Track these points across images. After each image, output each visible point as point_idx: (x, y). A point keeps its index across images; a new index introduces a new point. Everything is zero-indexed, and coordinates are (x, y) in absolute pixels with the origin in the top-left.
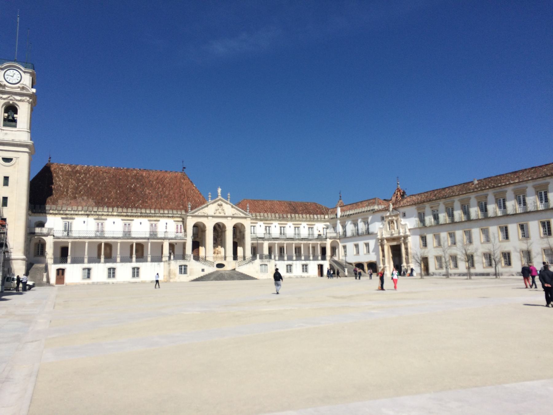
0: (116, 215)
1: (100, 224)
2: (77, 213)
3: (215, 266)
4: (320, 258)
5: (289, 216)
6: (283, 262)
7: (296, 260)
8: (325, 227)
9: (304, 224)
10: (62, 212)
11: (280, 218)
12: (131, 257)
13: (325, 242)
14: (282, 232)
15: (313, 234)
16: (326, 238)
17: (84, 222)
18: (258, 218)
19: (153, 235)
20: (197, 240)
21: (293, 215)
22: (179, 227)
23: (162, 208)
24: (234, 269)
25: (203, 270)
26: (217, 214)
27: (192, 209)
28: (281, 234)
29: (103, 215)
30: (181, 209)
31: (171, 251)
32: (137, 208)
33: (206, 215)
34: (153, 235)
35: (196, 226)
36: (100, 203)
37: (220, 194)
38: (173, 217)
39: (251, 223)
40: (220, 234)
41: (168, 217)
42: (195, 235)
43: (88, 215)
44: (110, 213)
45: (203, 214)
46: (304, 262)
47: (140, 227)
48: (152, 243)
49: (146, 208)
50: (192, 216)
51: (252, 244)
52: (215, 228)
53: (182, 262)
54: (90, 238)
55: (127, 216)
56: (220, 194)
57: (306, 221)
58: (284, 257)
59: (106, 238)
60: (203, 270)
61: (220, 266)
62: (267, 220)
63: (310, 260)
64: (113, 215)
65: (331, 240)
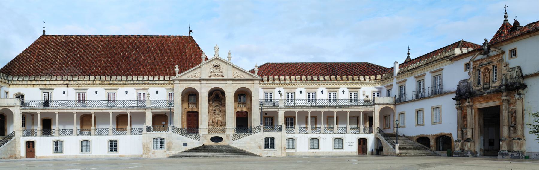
0: (97, 84)
1: (81, 94)
2: (56, 83)
8: (376, 90)
9: (343, 87)
10: (40, 82)
13: (370, 109)
15: (356, 100)
16: (374, 105)
17: (64, 92)
21: (327, 77)
29: (83, 84)
38: (164, 84)
41: (158, 84)
43: (67, 85)
44: (91, 82)
55: (112, 84)
64: (94, 84)
65: (382, 107)
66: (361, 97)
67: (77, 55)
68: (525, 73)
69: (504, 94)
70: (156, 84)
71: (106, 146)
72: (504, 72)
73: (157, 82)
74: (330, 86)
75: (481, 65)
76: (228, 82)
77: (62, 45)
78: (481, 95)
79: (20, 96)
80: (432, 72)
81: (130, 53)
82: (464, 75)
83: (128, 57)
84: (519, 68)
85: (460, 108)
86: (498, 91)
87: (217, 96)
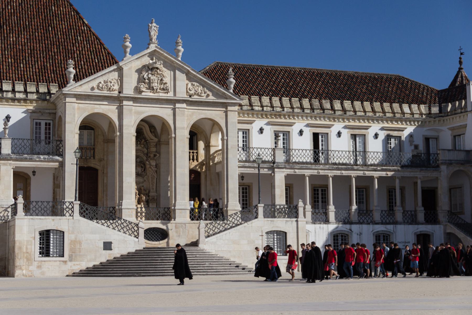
3: (142, 232)
4: (421, 216)
5: (337, 105)
6: (325, 226)
7: (359, 223)
11: (312, 109)
16: (438, 166)
18: (256, 108)
20: (93, 164)
24: (195, 244)
25: (108, 246)
26: (148, 94)
27: (77, 79)
30: (48, 82)
33: (115, 93)
35: (87, 126)
37: (154, 38)
38: (25, 100)
39: (239, 122)
40: (153, 149)
41: (13, 100)
42: (85, 150)
45: (105, 93)
46: (380, 228)
50: (79, 97)
51: (242, 177)
52: (139, 133)
53: (49, 222)
56: (154, 38)
57: (378, 120)
58: (326, 214)
60: (108, 246)
61: (152, 234)
62: (279, 115)
63: (395, 223)
70: (7, 100)
73: (10, 95)
74: (352, 123)
76: (178, 105)
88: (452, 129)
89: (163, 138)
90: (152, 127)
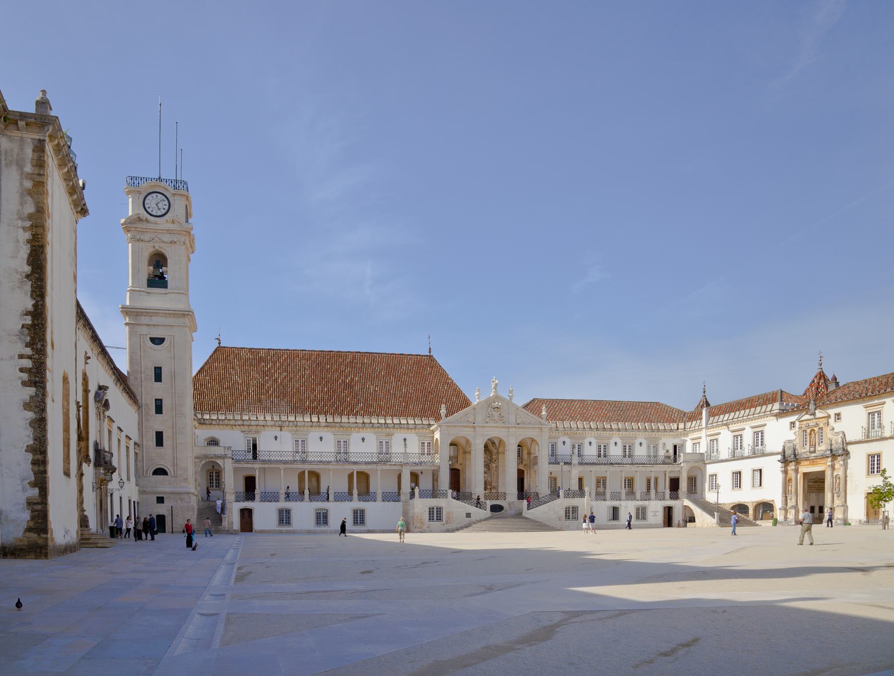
9: (641, 438)
12: (350, 493)
14: (602, 453)
17: (276, 438)
19: (384, 458)
20: (457, 466)
22: (426, 445)
23: (396, 416)
28: (599, 456)
31: (413, 485)
32: (356, 415)
34: (384, 458)
36: (298, 409)
38: (415, 428)
40: (494, 457)
41: (408, 428)
47: (363, 444)
48: (382, 470)
49: (370, 414)
52: (486, 447)
54: (285, 462)
59: (311, 462)
66: (662, 453)
67: (276, 380)
68: (848, 439)
69: (830, 459)
71: (275, 517)
72: (830, 436)
75: (808, 427)
77: (251, 364)
78: (807, 459)
79: (213, 442)
80: (752, 428)
81: (352, 379)
82: (791, 435)
83: (350, 386)
84: (843, 433)
85: (785, 472)
86: (824, 457)
87: (492, 449)
88: (692, 439)
89: (501, 450)
90: (493, 443)
